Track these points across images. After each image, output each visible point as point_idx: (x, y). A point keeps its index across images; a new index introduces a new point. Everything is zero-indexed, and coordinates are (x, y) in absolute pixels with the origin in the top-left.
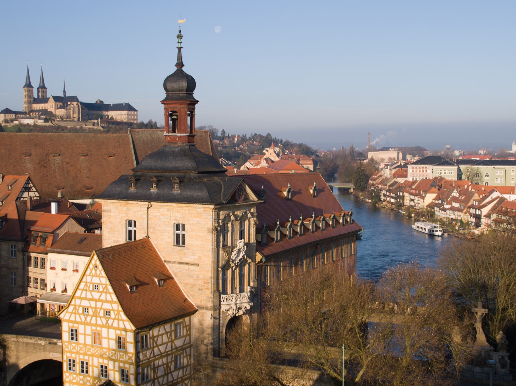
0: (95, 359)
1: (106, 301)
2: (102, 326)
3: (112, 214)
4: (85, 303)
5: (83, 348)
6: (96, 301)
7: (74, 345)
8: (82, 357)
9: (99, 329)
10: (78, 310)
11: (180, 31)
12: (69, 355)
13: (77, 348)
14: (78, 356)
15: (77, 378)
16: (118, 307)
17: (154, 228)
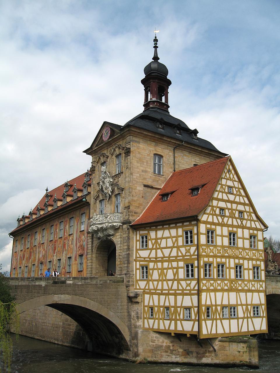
0: (232, 260)
1: (240, 203)
2: (238, 227)
3: (141, 146)
4: (222, 205)
5: (220, 250)
6: (232, 202)
7: (211, 248)
8: (219, 260)
9: (235, 229)
10: (215, 212)
11: (156, 37)
12: (206, 259)
13: (215, 251)
14: (215, 259)
15: (214, 285)
16: (250, 208)
17: (179, 165)
